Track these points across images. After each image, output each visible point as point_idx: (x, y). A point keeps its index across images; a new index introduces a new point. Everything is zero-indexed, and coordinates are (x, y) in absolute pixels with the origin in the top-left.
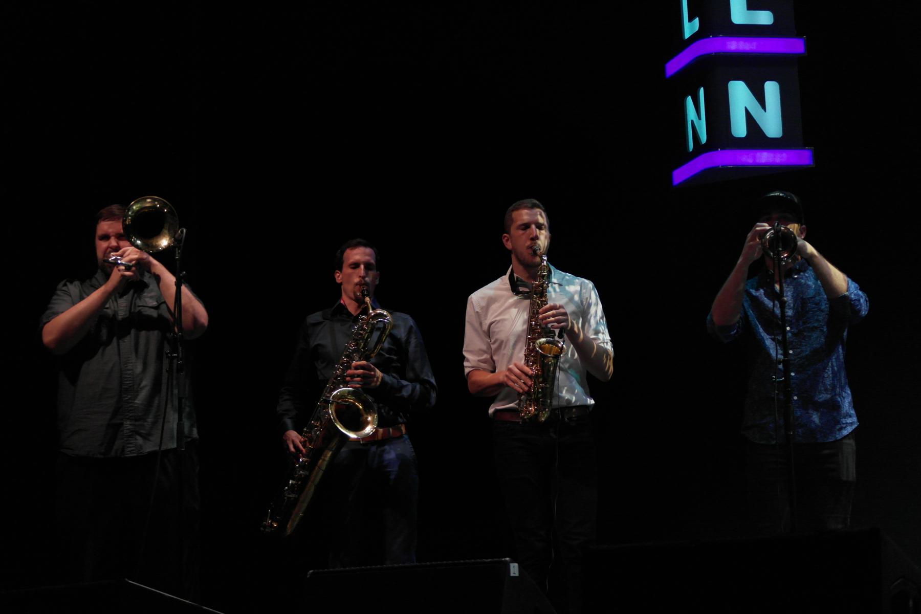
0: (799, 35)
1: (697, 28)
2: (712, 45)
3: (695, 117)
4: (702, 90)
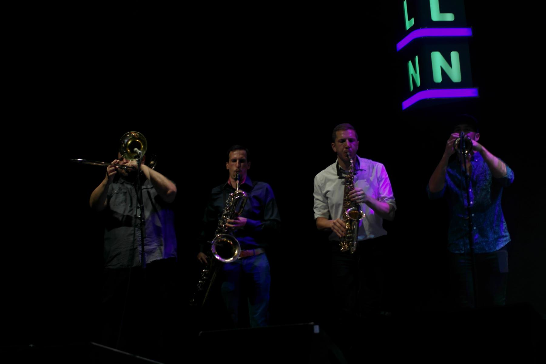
3: (414, 72)
4: (417, 58)
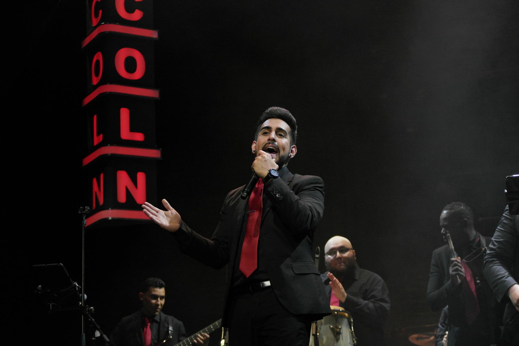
0: (158, 148)
1: (101, 140)
2: (110, 150)
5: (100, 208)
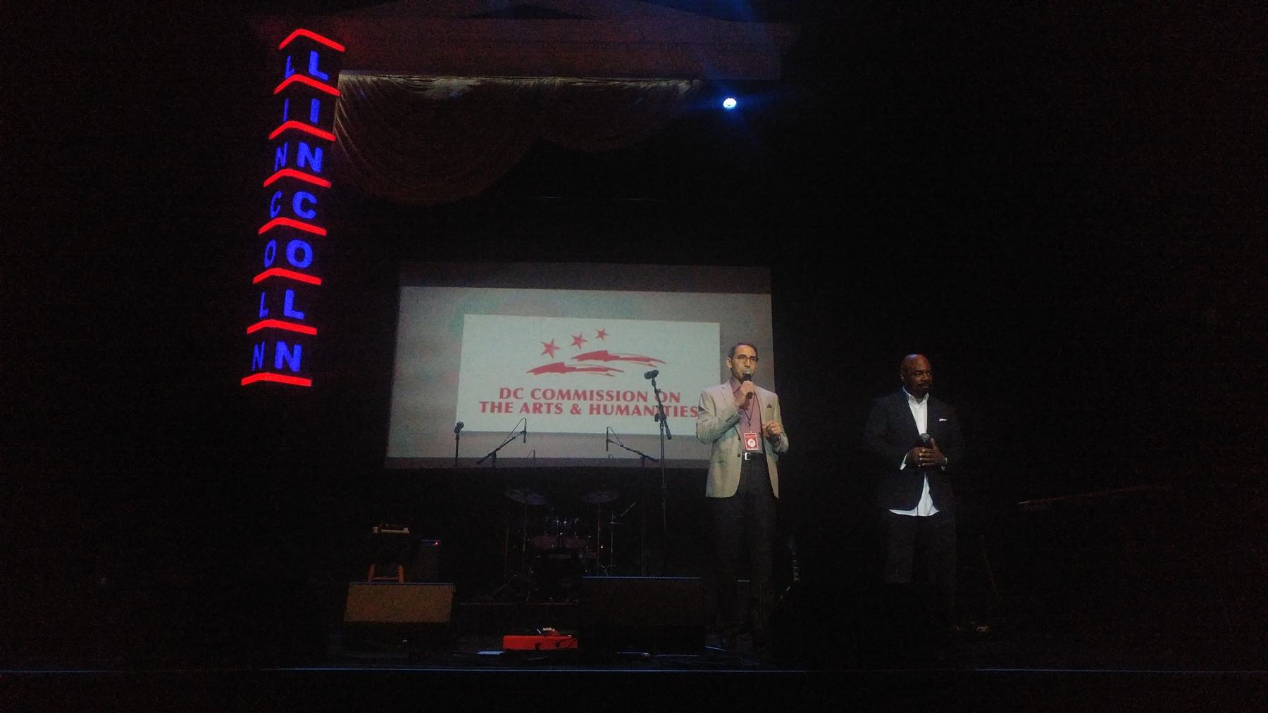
3: (258, 354)
5: (258, 371)
